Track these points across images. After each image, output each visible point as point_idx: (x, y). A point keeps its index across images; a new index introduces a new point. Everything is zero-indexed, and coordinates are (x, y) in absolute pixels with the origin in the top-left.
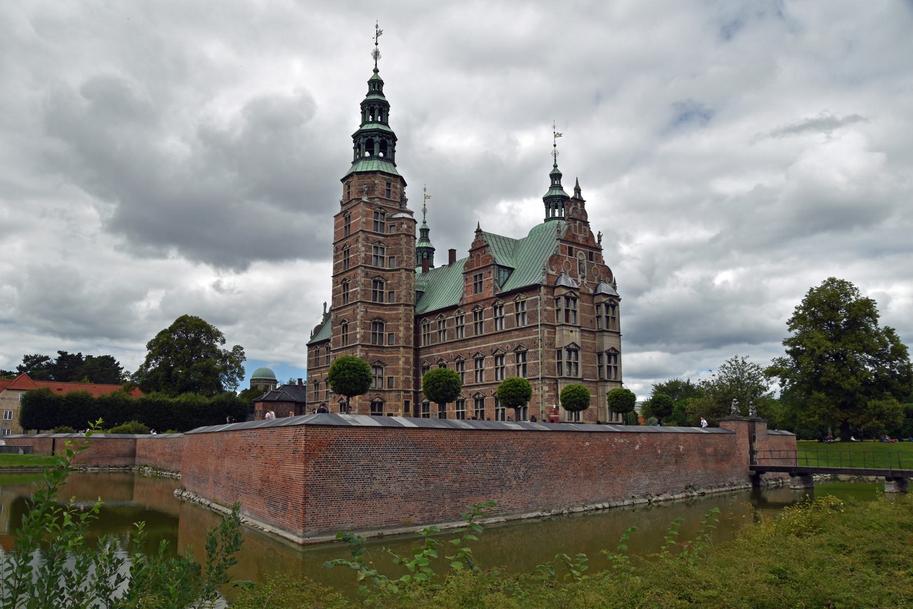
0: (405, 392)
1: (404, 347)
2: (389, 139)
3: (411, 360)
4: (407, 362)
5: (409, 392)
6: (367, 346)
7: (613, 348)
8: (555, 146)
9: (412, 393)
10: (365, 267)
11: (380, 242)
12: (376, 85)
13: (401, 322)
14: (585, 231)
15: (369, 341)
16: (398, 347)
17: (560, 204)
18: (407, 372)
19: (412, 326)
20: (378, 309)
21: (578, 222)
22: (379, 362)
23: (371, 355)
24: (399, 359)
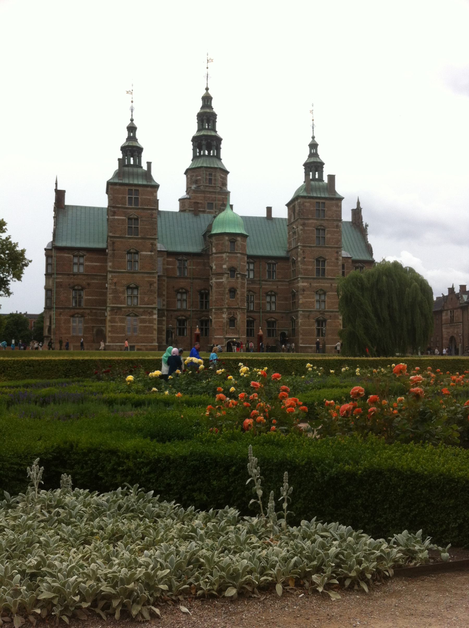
8: (132, 102)
12: (207, 100)
17: (129, 153)
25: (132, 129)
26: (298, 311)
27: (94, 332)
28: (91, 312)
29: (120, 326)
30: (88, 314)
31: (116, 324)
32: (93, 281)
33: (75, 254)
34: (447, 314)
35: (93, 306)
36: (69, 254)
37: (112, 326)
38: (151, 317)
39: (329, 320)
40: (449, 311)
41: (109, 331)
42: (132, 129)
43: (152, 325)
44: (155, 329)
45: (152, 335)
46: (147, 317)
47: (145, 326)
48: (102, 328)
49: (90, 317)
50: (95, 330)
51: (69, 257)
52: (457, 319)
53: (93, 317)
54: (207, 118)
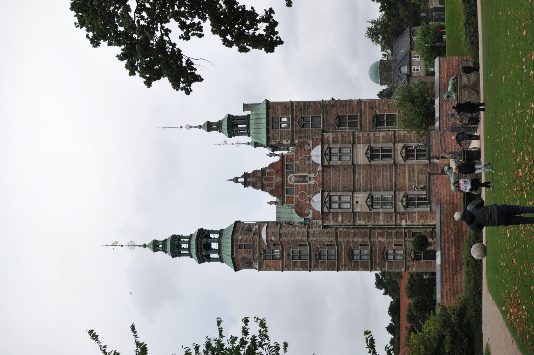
0: (405, 236)
1: (370, 238)
2: (201, 243)
3: (380, 231)
4: (381, 235)
5: (405, 233)
6: (372, 264)
7: (366, 153)
8: (181, 127)
9: (406, 231)
10: (310, 267)
11: (289, 255)
12: (156, 246)
13: (351, 240)
14: (270, 173)
15: (368, 263)
16: (370, 242)
18: (389, 235)
19: (353, 231)
20: (342, 255)
21: (264, 182)
22: (383, 254)
23: (378, 261)
24: (380, 241)
25: (209, 127)
42: (209, 127)
54: (175, 246)
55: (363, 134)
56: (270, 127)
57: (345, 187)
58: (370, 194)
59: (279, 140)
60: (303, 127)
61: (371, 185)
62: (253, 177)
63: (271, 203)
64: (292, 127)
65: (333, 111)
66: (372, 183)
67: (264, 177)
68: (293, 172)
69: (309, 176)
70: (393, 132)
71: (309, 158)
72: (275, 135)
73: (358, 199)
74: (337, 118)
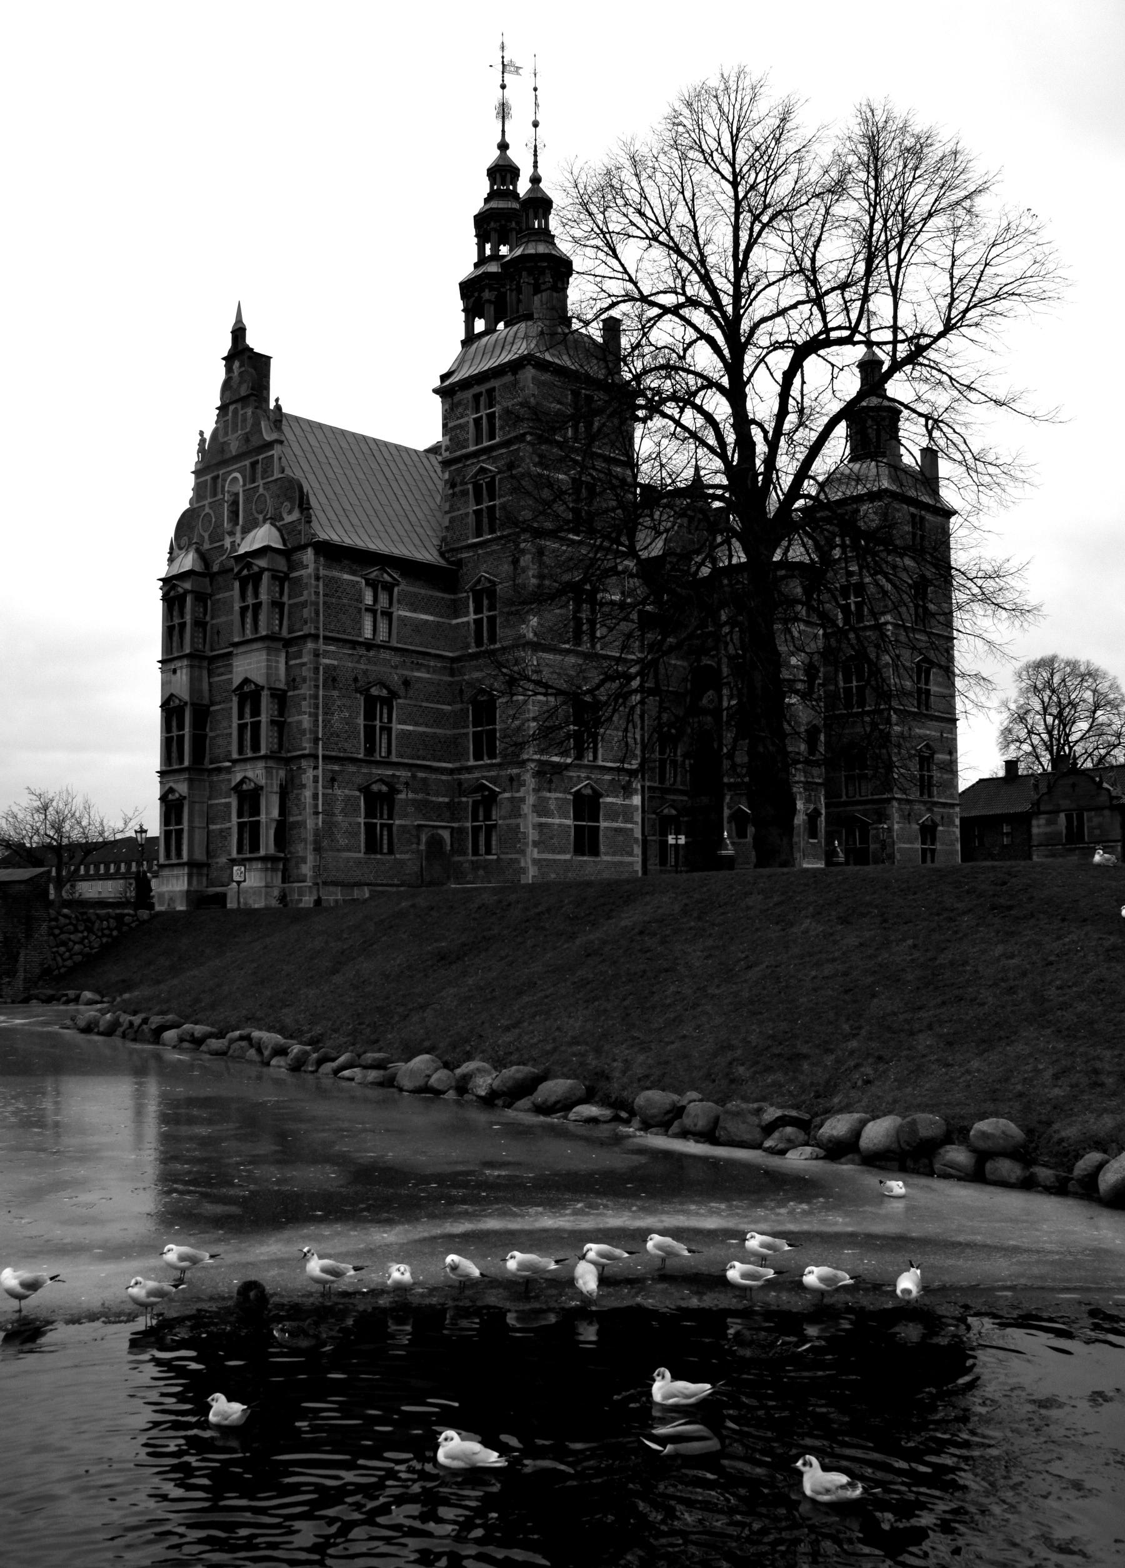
7: (246, 681)
8: (536, 124)
14: (244, 420)
21: (231, 408)
26: (889, 801)
27: (423, 847)
28: (414, 777)
29: (560, 825)
30: (407, 784)
31: (550, 820)
32: (417, 674)
33: (372, 576)
34: (1049, 823)
35: (418, 758)
36: (354, 573)
37: (541, 825)
38: (627, 802)
39: (940, 828)
40: (1062, 815)
41: (536, 844)
43: (630, 826)
44: (636, 839)
45: (630, 859)
46: (619, 801)
47: (616, 830)
48: (440, 832)
49: (411, 796)
50: (424, 838)
51: (355, 584)
52: (1097, 832)
53: (420, 796)
55: (304, 664)
56: (477, 389)
57: (218, 632)
58: (186, 703)
59: (450, 425)
60: (477, 488)
61: (220, 703)
62: (241, 374)
63: (203, 441)
64: (475, 454)
65: (506, 566)
66: (222, 706)
67: (239, 406)
68: (244, 485)
69: (239, 528)
70: (307, 752)
71: (264, 521)
72: (460, 410)
73: (178, 672)
74: (490, 581)
